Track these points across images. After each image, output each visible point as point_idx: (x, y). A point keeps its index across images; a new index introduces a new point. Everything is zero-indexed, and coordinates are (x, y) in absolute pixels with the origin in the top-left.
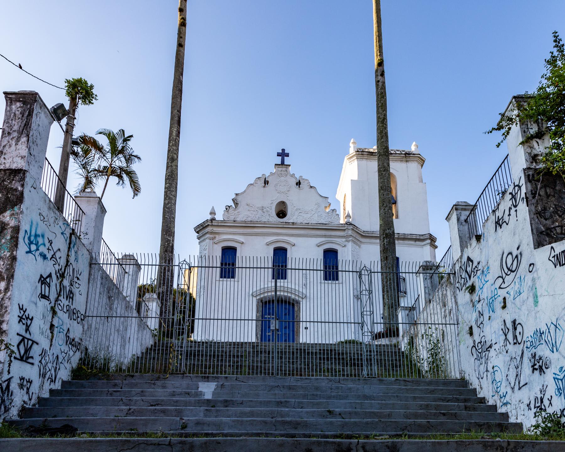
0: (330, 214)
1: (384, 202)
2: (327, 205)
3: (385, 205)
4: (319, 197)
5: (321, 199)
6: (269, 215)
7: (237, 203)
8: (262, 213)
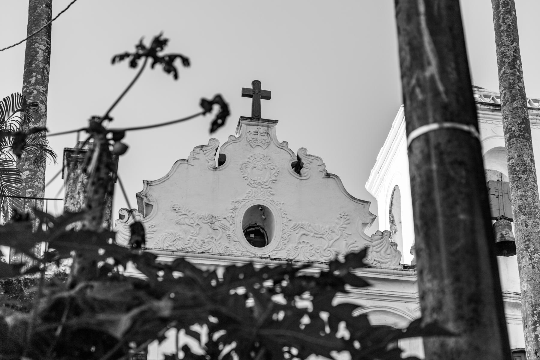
0: (376, 242)
1: (529, 240)
2: (368, 219)
4: (348, 200)
5: (352, 204)
6: (229, 236)
7: (147, 205)
8: (211, 231)
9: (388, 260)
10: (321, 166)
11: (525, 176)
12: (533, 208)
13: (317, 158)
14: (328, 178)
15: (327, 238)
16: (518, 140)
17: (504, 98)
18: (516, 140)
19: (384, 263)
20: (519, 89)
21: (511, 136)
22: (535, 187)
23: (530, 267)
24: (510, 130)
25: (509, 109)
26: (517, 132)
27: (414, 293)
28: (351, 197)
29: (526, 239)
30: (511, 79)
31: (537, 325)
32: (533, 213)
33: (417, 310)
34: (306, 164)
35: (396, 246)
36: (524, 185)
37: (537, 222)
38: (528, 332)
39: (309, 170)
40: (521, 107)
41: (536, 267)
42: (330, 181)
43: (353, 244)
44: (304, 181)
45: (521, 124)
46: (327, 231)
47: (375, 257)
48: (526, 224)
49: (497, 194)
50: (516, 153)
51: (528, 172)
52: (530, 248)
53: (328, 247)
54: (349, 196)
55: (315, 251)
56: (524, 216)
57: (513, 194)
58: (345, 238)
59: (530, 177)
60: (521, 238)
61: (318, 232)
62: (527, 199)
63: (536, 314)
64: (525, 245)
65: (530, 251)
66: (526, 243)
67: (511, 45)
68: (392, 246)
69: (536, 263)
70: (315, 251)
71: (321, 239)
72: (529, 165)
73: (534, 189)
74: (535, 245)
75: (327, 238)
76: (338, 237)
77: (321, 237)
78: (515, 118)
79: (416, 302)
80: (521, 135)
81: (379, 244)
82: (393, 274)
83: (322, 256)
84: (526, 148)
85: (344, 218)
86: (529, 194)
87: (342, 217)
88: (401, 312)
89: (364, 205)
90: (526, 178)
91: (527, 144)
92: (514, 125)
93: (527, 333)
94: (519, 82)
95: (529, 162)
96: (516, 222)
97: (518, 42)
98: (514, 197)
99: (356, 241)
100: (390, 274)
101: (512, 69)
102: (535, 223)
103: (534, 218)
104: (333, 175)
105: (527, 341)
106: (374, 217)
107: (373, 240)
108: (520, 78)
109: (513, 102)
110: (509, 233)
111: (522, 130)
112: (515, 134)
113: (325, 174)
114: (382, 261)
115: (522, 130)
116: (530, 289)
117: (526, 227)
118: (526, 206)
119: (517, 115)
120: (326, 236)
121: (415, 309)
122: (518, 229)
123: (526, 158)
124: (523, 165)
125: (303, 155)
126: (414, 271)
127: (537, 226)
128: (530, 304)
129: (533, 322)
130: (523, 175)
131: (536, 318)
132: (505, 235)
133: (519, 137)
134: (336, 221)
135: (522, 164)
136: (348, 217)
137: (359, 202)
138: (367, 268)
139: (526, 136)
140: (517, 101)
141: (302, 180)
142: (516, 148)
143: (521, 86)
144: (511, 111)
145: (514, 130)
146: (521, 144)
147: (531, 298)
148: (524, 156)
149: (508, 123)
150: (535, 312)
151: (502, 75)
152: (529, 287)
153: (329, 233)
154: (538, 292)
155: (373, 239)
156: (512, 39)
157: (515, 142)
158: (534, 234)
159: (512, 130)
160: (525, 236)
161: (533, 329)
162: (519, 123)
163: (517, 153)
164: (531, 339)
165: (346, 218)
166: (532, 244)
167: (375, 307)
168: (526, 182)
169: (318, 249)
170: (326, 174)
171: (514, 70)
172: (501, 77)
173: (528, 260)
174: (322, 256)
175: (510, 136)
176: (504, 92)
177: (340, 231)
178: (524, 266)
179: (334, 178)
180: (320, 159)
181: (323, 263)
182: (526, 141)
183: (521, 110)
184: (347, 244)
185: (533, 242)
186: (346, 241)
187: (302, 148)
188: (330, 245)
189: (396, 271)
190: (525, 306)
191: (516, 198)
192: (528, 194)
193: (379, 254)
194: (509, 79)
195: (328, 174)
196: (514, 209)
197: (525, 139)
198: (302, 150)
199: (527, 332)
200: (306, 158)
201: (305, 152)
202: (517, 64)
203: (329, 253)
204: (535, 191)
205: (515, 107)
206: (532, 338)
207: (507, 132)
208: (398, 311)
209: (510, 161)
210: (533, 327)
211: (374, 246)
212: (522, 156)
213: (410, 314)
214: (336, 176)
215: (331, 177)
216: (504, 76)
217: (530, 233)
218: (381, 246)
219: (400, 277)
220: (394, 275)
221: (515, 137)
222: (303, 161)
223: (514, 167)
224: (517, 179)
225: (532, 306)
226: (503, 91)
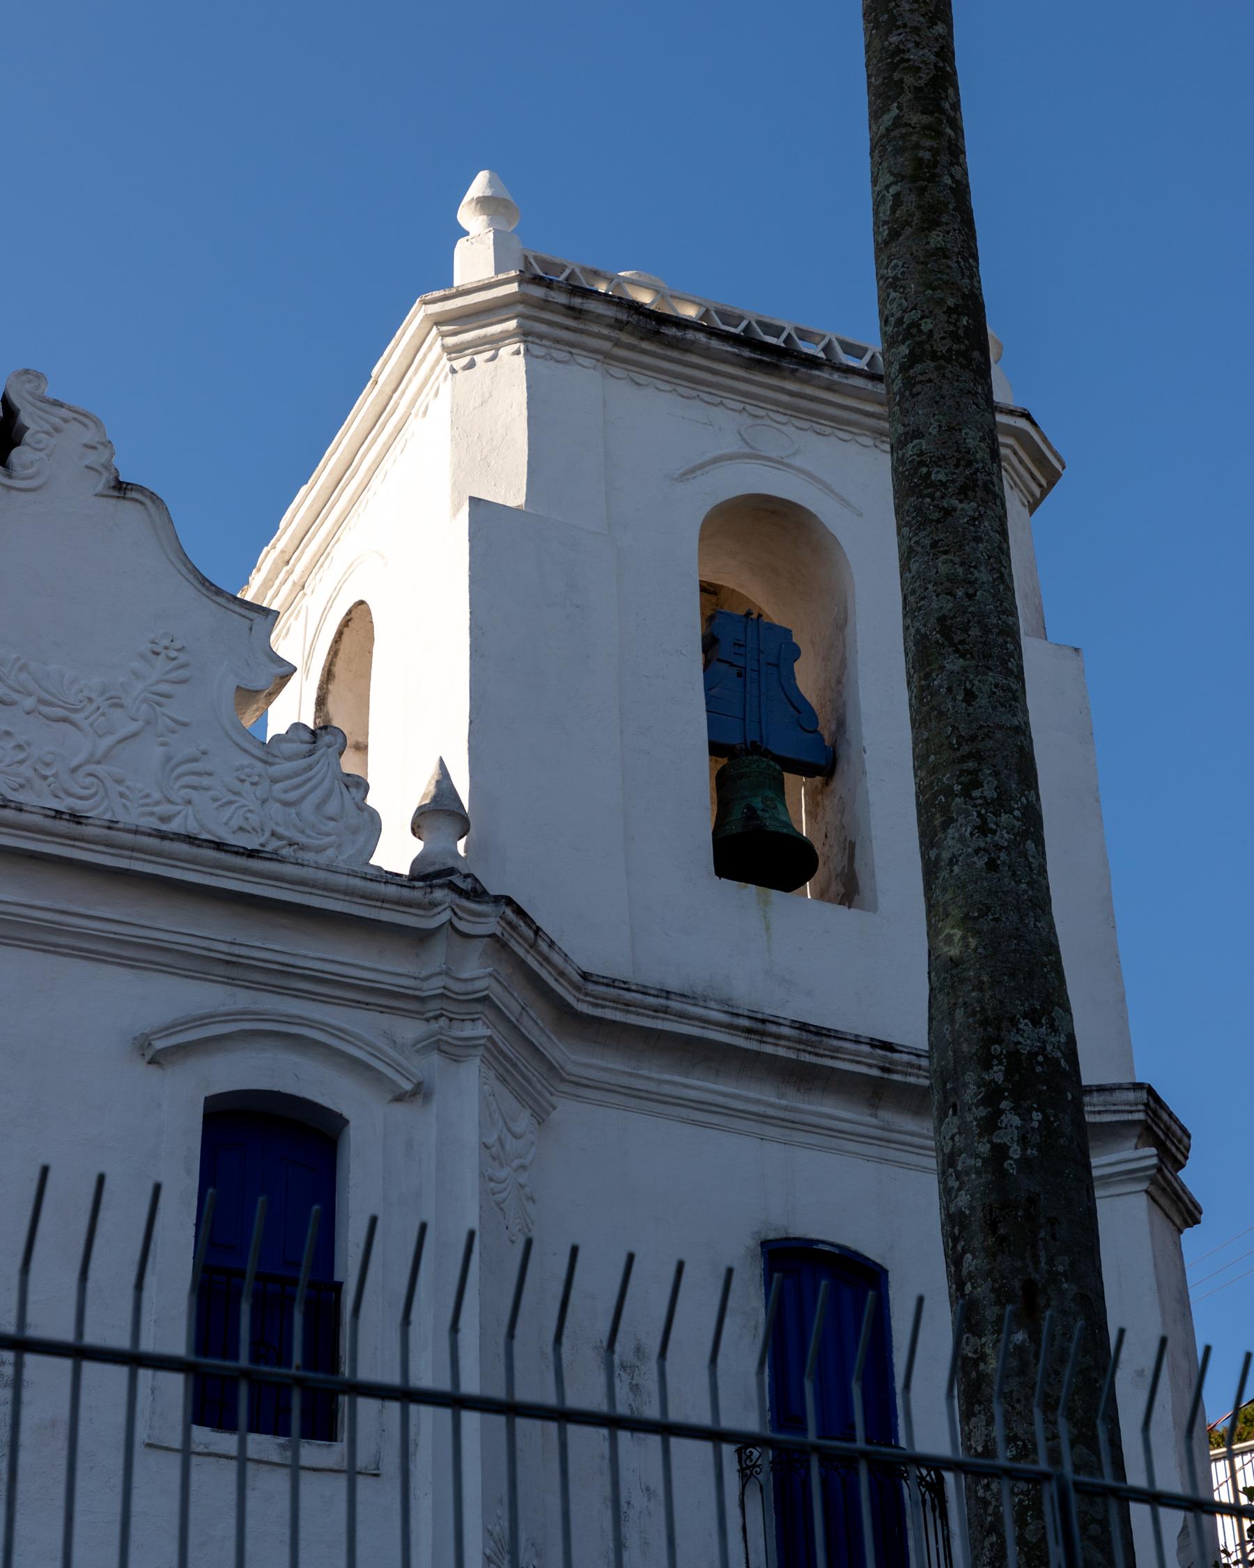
3: (988, 791)
9: (326, 840)
10: (94, 448)
11: (969, 507)
12: (995, 631)
13: (83, 417)
14: (118, 497)
15: (91, 725)
16: (944, 368)
17: (893, 210)
18: (938, 368)
19: (310, 851)
20: (951, 188)
21: (917, 351)
22: (1003, 553)
23: (980, 862)
24: (914, 331)
25: (912, 254)
26: (943, 338)
27: (421, 976)
28: (205, 582)
29: (966, 749)
30: (924, 148)
31: (1004, 1105)
32: (996, 651)
33: (424, 1046)
34: (38, 432)
35: (362, 790)
36: (965, 539)
37: (1010, 689)
38: (960, 1133)
39: (46, 458)
40: (959, 253)
41: (1004, 863)
42: (128, 511)
43: (194, 760)
44: (23, 496)
45: (959, 314)
46: (90, 700)
47: (277, 824)
48: (965, 689)
49: (740, 662)
50: (936, 417)
51: (980, 493)
52: (983, 786)
53: (88, 761)
54: (195, 576)
55: (35, 770)
56: (962, 660)
57: (914, 573)
58: (162, 735)
59: (989, 512)
60: (942, 745)
61: (53, 695)
62: (975, 594)
63: (998, 1057)
64: (962, 772)
65: (981, 798)
66: (965, 766)
67: (929, 28)
68: (347, 787)
69: (1003, 847)
70: (35, 770)
71: (67, 725)
72: (983, 467)
73: (1001, 562)
74: (1003, 776)
75: (91, 725)
76: (134, 726)
77: (65, 720)
78: (934, 289)
79: (423, 1014)
80: (958, 352)
81: (296, 774)
82: (346, 894)
83: (62, 794)
84: (974, 403)
85: (167, 657)
86: (983, 575)
87: (157, 654)
88: (361, 1048)
89: (251, 620)
90: (971, 513)
91: (980, 390)
92: (931, 312)
93: (957, 1138)
94: (952, 164)
95: (986, 456)
96: (923, 682)
97: (949, 25)
98: (918, 584)
99: (204, 753)
100: (333, 891)
101: (931, 113)
102: (1004, 691)
103: (1000, 673)
104: (141, 489)
105: (951, 1170)
106: (284, 670)
107: (276, 756)
108: (956, 151)
109: (930, 229)
110: (776, 807)
111: (962, 335)
112: (932, 346)
113: (108, 481)
114: (302, 839)
115: (962, 335)
116: (975, 950)
117: (969, 704)
118: (969, 621)
119: (944, 277)
120: (86, 719)
121: (419, 1042)
122: (933, 708)
123: (971, 438)
124: (963, 463)
125: (32, 400)
126: (428, 890)
127: (1010, 706)
128: (974, 1013)
129: (983, 1089)
130: (961, 502)
131: (1001, 1074)
132: (763, 810)
133: (949, 360)
134: (136, 665)
135: (958, 460)
136: (183, 658)
137: (231, 606)
138: (244, 858)
139: (975, 359)
140: (946, 228)
141: (14, 493)
142: (938, 398)
143: (958, 177)
144: (922, 259)
145: (931, 331)
146: (956, 384)
147: (981, 990)
148: (968, 430)
149: (905, 304)
150: (995, 1049)
151: (887, 129)
152: (973, 942)
153: (99, 708)
154: (1010, 965)
155: (276, 752)
156: (932, 8)
157: (934, 376)
158: (999, 735)
159: (920, 331)
160: (960, 737)
161: (982, 1118)
162: (949, 307)
163: (941, 417)
164: (971, 1162)
165: (174, 659)
166: (989, 772)
167: (260, 1016)
168: (972, 528)
169: (47, 765)
170: (113, 484)
171: (937, 118)
172: (882, 136)
173: (972, 834)
174: (62, 794)
175: (912, 352)
176: (893, 190)
177: (145, 706)
178: (951, 860)
179: (142, 503)
180: (95, 423)
181: (64, 816)
182: (975, 379)
183: (958, 262)
184: (168, 759)
185: (994, 766)
186: (164, 744)
187: (27, 371)
188: (99, 754)
189: (359, 883)
190: (952, 1022)
191: (930, 586)
192: (976, 574)
193: (293, 810)
194: (917, 146)
195: (121, 483)
196: (918, 630)
197: (972, 370)
198: (24, 378)
199: (956, 1130)
200: (40, 409)
201: (38, 387)
202: (947, 97)
203: (93, 785)
204: (1003, 569)
205: (937, 249)
206: (978, 1156)
207: (901, 337)
208: (350, 1042)
209: (910, 446)
210: (982, 1112)
211: (275, 781)
212: (960, 430)
213: (400, 1059)
214: (153, 496)
215: (129, 494)
216: (892, 134)
217: (984, 727)
218: (305, 782)
219: (372, 910)
220: (347, 898)
221: (934, 356)
222: (25, 418)
223: (924, 470)
224: (936, 516)
225: (985, 1023)
226: (887, 187)
